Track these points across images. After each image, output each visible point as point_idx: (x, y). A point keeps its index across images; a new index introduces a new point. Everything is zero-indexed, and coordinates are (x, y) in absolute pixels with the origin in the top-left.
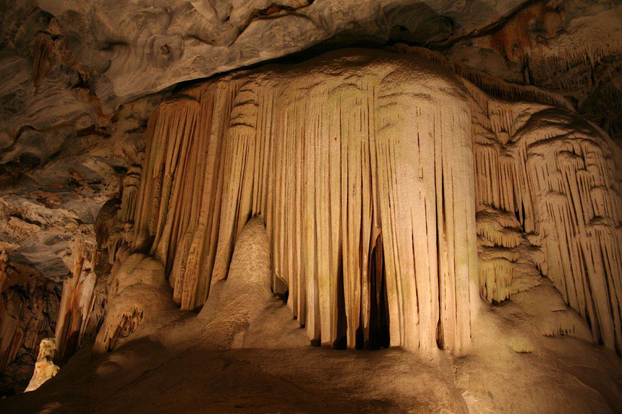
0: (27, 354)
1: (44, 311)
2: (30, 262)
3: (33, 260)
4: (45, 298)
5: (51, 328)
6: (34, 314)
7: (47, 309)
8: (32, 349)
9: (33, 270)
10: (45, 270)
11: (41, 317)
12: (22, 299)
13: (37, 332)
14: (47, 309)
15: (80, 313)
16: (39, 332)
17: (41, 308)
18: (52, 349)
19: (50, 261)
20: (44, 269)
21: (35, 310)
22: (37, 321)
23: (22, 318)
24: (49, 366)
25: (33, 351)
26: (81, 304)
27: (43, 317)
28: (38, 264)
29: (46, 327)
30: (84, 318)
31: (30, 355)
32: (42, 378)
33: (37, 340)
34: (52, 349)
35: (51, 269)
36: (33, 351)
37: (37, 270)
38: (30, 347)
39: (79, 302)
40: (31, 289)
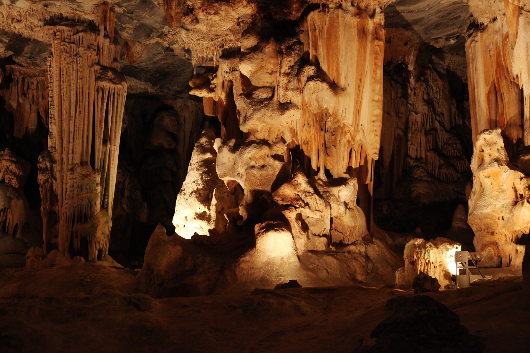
0: (417, 166)
1: (425, 97)
2: (405, 20)
3: (409, 17)
4: (422, 78)
5: (439, 122)
6: (412, 105)
7: (428, 94)
8: (421, 158)
9: (408, 34)
10: (426, 30)
11: (422, 107)
12: (391, 85)
13: (423, 131)
14: (428, 94)
15: (518, 86)
16: (425, 131)
17: (420, 93)
18: (500, 148)
19: (439, 11)
20: (426, 29)
21: (412, 98)
22: (419, 115)
23: (397, 113)
24: (504, 174)
25: (424, 161)
26: (515, 71)
27: (426, 107)
28: (417, 22)
29: (432, 123)
30: (526, 94)
31: (423, 167)
32: (497, 193)
33: (426, 144)
34: (500, 148)
35: (437, 26)
36: (424, 161)
37: (414, 32)
38: (419, 156)
39: (511, 66)
40: (409, 66)
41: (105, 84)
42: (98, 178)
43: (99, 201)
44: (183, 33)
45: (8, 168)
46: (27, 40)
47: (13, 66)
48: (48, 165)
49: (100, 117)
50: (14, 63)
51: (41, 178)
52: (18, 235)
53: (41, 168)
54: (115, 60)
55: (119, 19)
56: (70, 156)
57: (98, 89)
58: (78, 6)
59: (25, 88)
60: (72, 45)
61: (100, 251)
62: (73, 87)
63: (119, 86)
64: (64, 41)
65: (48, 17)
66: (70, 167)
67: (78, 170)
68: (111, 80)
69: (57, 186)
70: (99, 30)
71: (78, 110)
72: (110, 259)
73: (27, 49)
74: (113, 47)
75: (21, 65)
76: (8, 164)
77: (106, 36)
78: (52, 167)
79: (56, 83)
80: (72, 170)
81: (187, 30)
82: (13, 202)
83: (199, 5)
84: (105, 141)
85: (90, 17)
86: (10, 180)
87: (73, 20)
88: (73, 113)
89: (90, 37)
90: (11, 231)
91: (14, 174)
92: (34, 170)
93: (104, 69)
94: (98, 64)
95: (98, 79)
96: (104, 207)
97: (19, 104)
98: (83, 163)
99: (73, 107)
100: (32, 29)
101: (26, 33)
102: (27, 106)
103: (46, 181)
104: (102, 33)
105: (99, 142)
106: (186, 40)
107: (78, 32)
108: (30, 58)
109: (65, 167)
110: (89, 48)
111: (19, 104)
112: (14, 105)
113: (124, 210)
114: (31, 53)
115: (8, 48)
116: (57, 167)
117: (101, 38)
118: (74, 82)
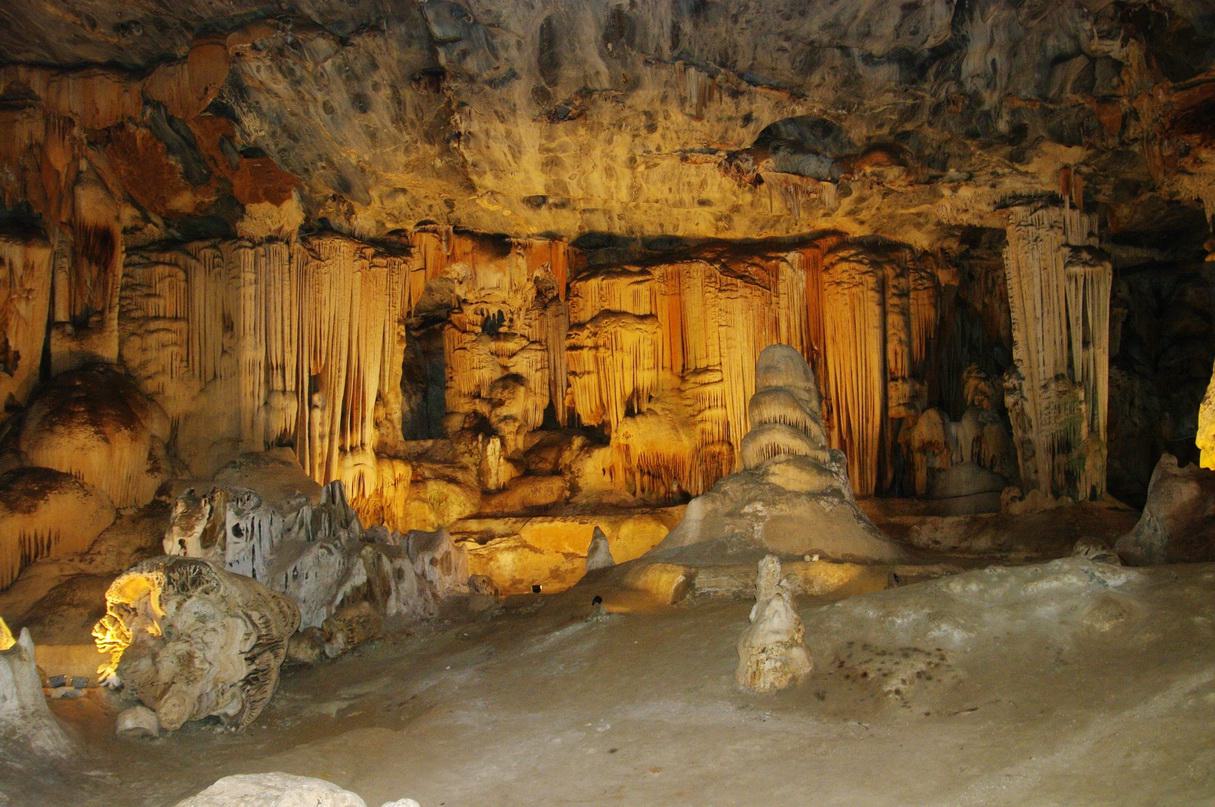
41: (1078, 270)
42: (1082, 395)
43: (1084, 425)
44: (1186, 180)
45: (976, 388)
46: (982, 230)
47: (972, 262)
48: (1016, 382)
49: (1076, 313)
50: (972, 258)
51: (1009, 400)
52: (996, 470)
53: (1008, 390)
54: (1091, 234)
55: (1090, 181)
56: (1041, 369)
57: (1069, 277)
58: (1033, 178)
59: (990, 281)
60: (1030, 228)
61: (1093, 489)
62: (1037, 280)
63: (1099, 268)
64: (1019, 225)
65: (998, 200)
66: (1043, 383)
67: (1053, 386)
68: (1085, 263)
69: (1028, 407)
70: (1063, 202)
71: (1046, 309)
72: (1110, 498)
73: (984, 238)
74: (1085, 219)
75: (982, 259)
76: (976, 382)
77: (1073, 207)
78: (1020, 385)
79: (1015, 280)
80: (1045, 387)
81: (1191, 174)
82: (986, 429)
83: (1198, 141)
84: (1086, 344)
85: (1049, 189)
86: (981, 401)
87: (1029, 196)
88: (1039, 314)
89: (1050, 214)
90: (988, 465)
91: (983, 393)
92: (1002, 393)
93: (1076, 250)
94: (1067, 245)
95: (1069, 264)
96: (1093, 429)
97: (985, 305)
98: (1058, 377)
99: (1038, 306)
100: (981, 217)
101: (976, 222)
102: (996, 305)
103: (1016, 403)
104: (1067, 205)
105: (1077, 345)
106: (1192, 188)
107: (1035, 211)
108: (990, 248)
109: (1036, 382)
110: (1052, 227)
111: (985, 305)
112: (979, 307)
113: (1135, 424)
114: (990, 242)
115: (962, 242)
116: (1026, 385)
117: (1067, 211)
118: (1037, 273)
